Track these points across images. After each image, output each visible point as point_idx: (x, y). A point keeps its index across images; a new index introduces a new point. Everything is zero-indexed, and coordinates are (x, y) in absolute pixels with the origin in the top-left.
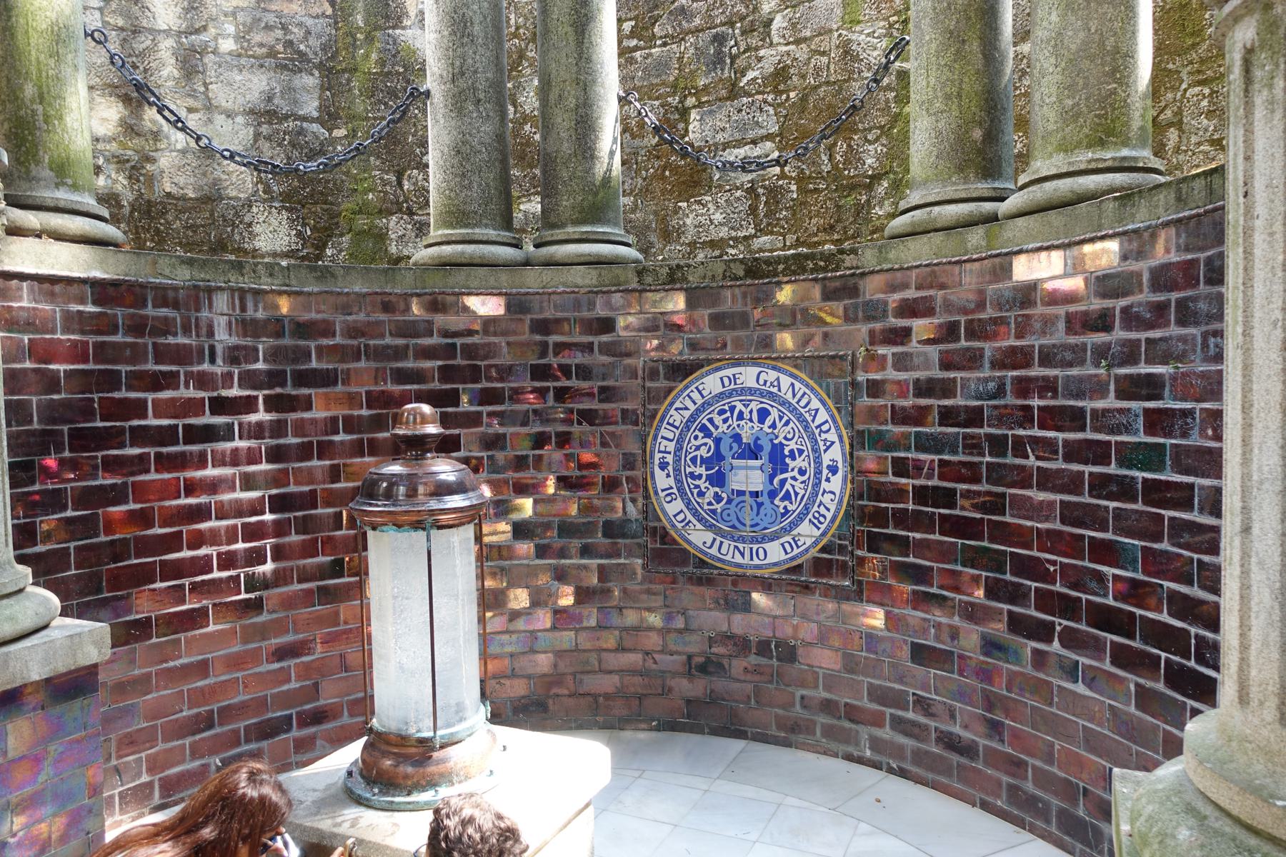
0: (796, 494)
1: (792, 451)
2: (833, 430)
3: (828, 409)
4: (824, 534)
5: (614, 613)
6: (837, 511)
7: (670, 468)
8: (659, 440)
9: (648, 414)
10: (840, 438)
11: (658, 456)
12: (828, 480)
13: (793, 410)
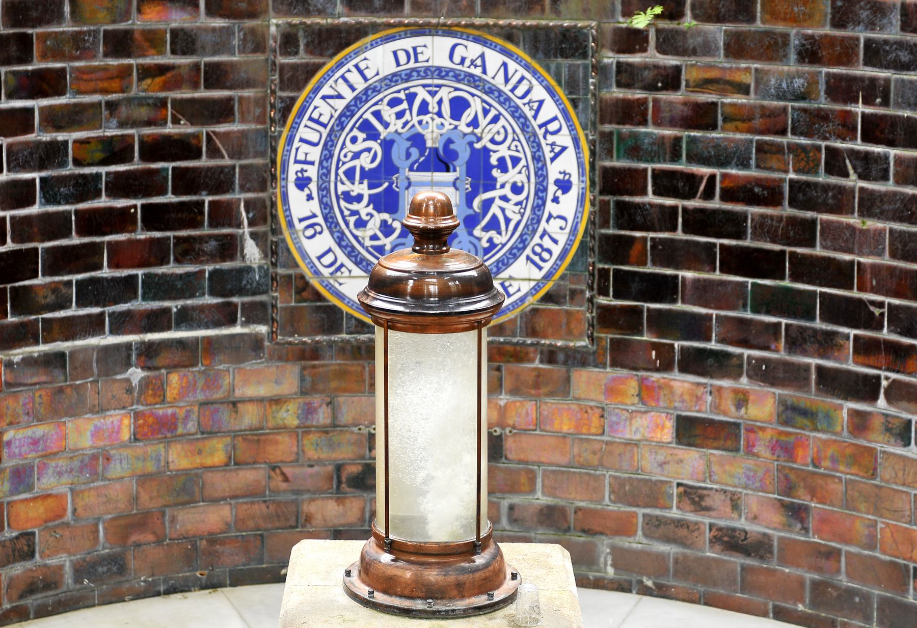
0: (508, 221)
1: (502, 160)
3: (558, 102)
6: (570, 243)
7: (313, 186)
8: (296, 143)
11: (293, 168)
12: (556, 200)
13: (504, 100)
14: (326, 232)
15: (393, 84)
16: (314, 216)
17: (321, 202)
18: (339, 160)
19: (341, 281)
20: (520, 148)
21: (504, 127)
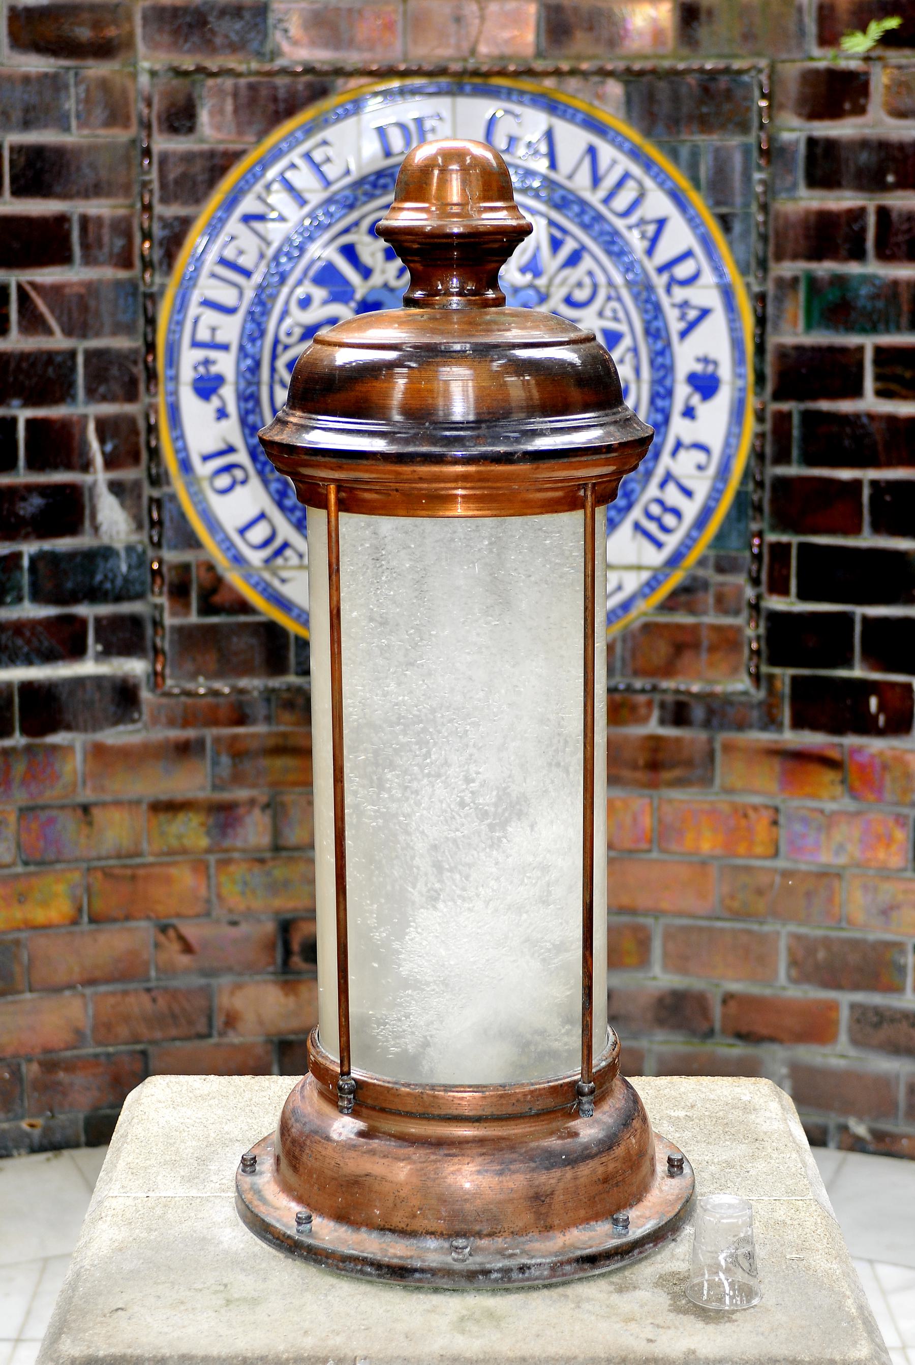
2: (708, 277)
3: (693, 222)
4: (675, 560)
5: (68, 825)
6: (715, 494)
7: (228, 393)
8: (193, 310)
9: (158, 232)
10: (727, 293)
11: (189, 358)
12: (689, 413)
13: (591, 220)
14: (255, 482)
15: (378, 192)
16: (231, 450)
17: (243, 422)
18: (276, 342)
19: (285, 574)
20: (621, 314)
21: (590, 273)
